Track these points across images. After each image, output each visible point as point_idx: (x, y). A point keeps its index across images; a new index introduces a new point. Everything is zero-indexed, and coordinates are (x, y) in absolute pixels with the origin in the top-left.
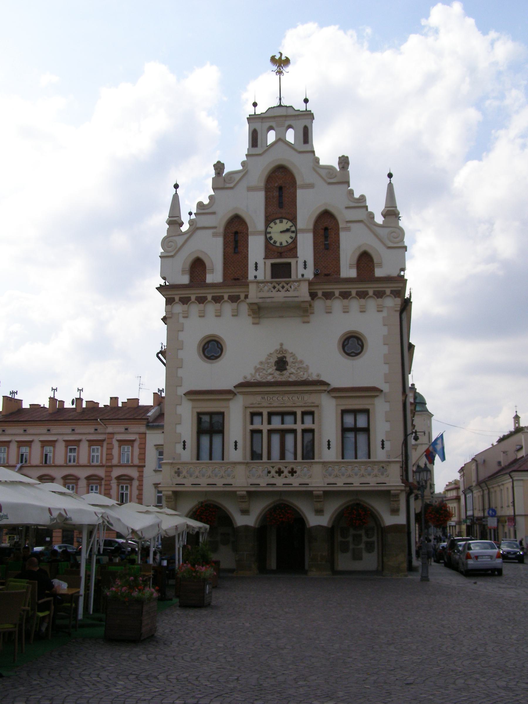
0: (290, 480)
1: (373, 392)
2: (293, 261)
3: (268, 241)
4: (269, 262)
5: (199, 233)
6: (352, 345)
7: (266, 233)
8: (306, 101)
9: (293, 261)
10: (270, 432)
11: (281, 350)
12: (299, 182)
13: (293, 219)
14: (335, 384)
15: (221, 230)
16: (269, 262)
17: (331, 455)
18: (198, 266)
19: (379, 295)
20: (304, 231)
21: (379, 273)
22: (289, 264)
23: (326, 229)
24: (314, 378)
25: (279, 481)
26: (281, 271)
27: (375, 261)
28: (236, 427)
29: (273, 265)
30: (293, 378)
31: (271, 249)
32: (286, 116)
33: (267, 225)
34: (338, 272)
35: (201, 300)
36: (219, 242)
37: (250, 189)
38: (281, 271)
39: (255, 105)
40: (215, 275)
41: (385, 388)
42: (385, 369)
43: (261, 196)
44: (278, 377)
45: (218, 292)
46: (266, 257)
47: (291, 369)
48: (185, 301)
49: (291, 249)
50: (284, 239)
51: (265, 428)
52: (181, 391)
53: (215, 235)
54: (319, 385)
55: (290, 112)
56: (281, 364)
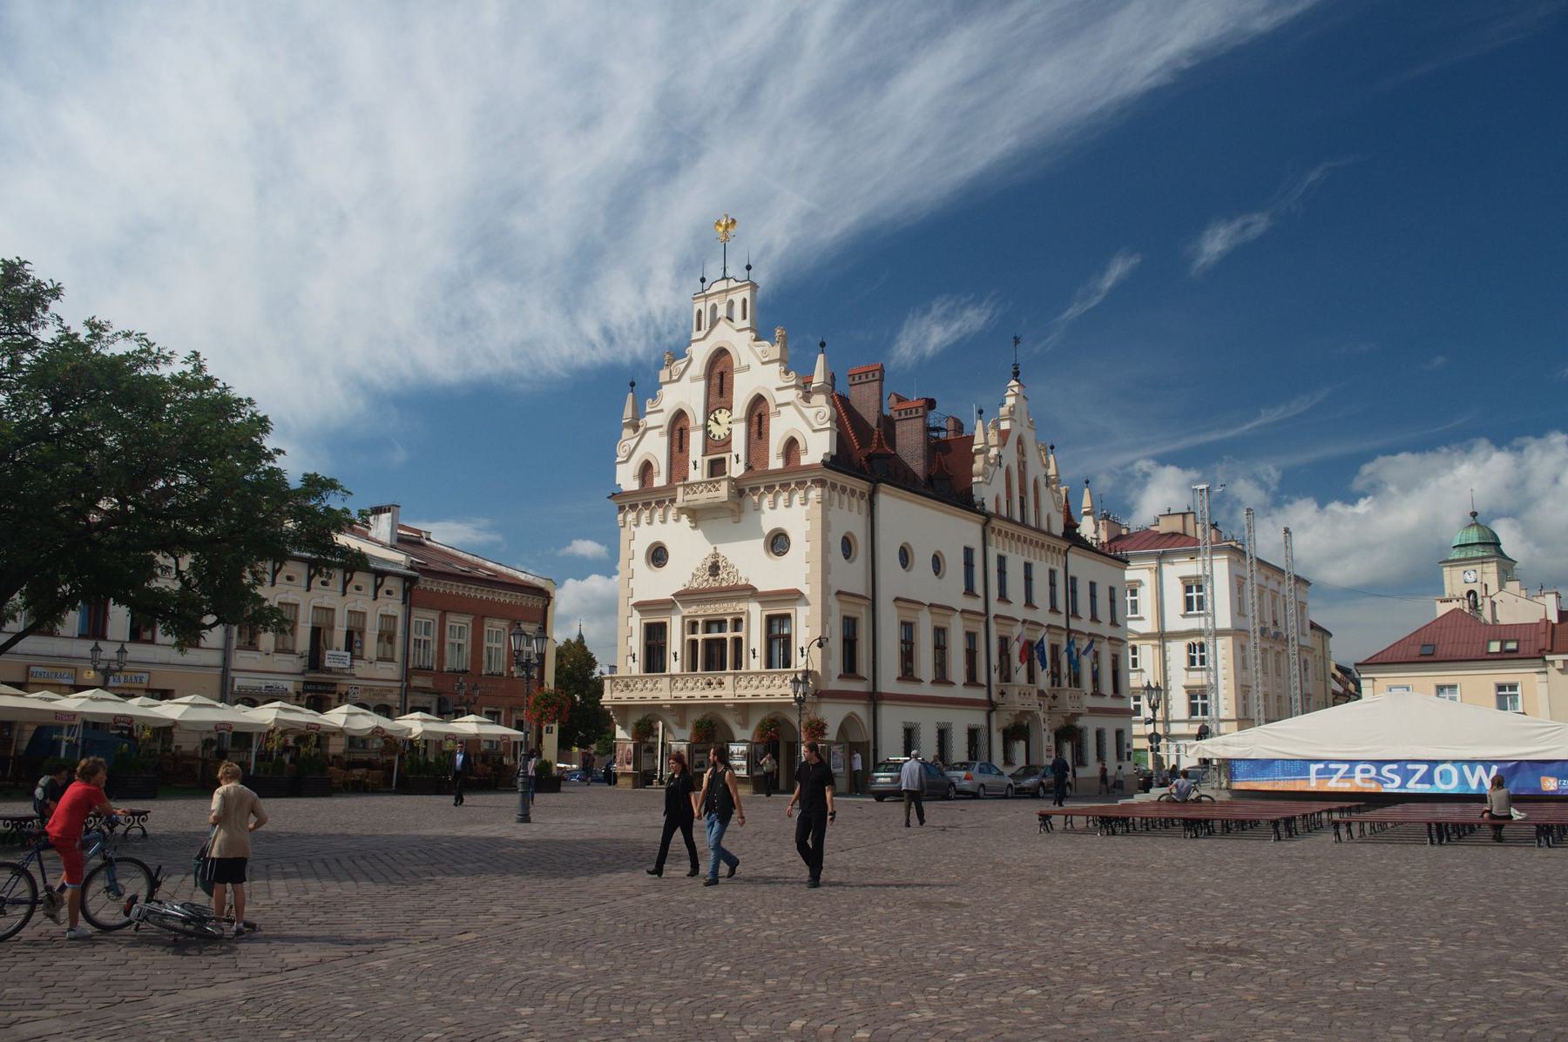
0: (718, 692)
1: (795, 596)
2: (727, 456)
3: (707, 433)
4: (707, 458)
5: (649, 433)
6: (778, 543)
7: (706, 426)
8: (749, 268)
9: (727, 456)
10: (708, 642)
11: (716, 555)
12: (736, 365)
13: (730, 409)
14: (761, 589)
15: (665, 429)
16: (707, 458)
17: (756, 664)
18: (646, 469)
19: (801, 484)
20: (737, 420)
21: (805, 460)
22: (723, 460)
23: (760, 416)
24: (743, 582)
25: (711, 693)
26: (716, 468)
27: (802, 446)
28: (675, 641)
29: (712, 463)
30: (724, 584)
31: (710, 444)
32: (727, 291)
33: (707, 418)
34: (767, 463)
35: (647, 505)
36: (665, 440)
37: (693, 380)
38: (716, 468)
39: (703, 280)
40: (660, 481)
41: (806, 590)
42: (807, 569)
43: (701, 386)
44: (712, 583)
45: (659, 496)
46: (705, 453)
47: (723, 574)
48: (633, 507)
49: (726, 443)
50: (718, 431)
51: (700, 636)
52: (632, 601)
53: (661, 434)
54: (749, 592)
55: (732, 284)
56: (714, 569)
